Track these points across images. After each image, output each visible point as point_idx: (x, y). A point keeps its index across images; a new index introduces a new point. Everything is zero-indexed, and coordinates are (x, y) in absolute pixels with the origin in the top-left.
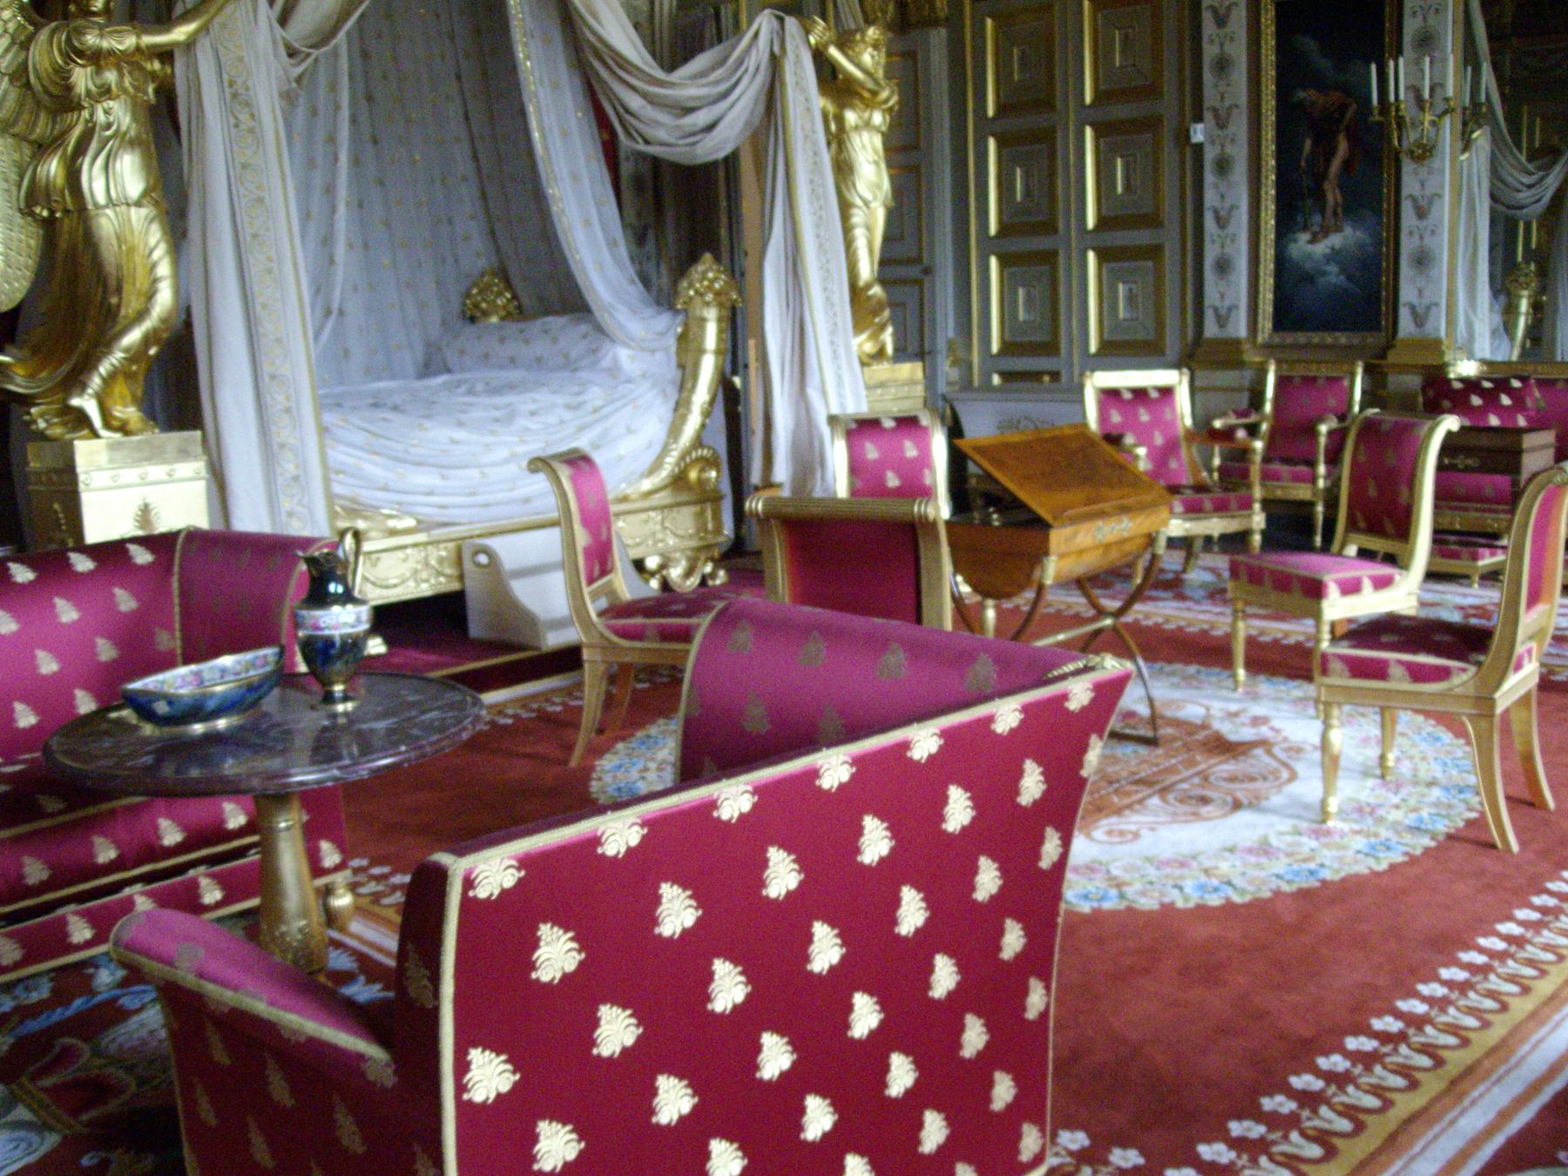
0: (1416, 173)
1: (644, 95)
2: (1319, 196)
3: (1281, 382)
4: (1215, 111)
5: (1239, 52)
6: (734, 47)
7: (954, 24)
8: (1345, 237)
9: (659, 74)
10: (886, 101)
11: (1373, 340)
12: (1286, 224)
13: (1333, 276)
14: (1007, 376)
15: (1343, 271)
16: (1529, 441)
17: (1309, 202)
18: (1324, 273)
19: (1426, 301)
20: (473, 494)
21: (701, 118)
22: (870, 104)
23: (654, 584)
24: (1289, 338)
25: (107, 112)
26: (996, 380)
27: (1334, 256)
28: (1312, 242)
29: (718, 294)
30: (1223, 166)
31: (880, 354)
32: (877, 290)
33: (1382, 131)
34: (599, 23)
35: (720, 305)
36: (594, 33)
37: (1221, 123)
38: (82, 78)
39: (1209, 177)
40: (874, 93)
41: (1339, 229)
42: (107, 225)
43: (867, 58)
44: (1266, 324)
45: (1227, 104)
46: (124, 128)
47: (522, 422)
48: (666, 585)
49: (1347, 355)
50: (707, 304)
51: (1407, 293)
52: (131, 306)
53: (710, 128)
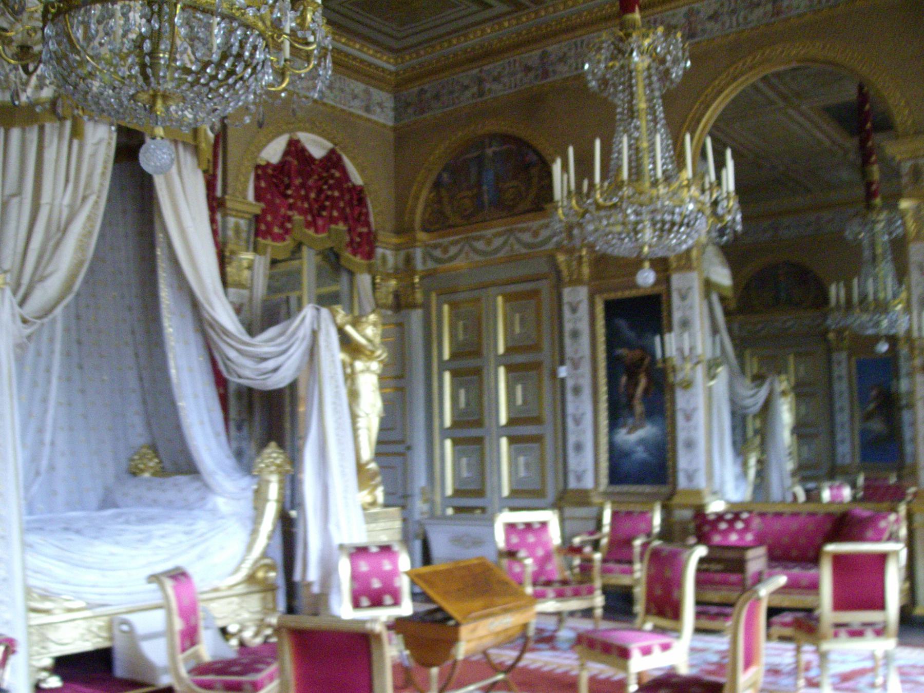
1: (238, 350)
2: (630, 406)
3: (615, 515)
5: (584, 326)
6: (290, 325)
7: (426, 306)
8: (647, 431)
9: (246, 338)
10: (379, 357)
11: (665, 490)
12: (614, 423)
13: (641, 454)
14: (458, 510)
16: (750, 554)
20: (121, 587)
21: (270, 364)
22: (370, 357)
23: (234, 642)
24: (618, 488)
26: (450, 511)
27: (641, 442)
29: (279, 466)
30: (577, 390)
31: (373, 504)
32: (373, 466)
33: (663, 373)
34: (213, 308)
35: (280, 473)
36: (208, 313)
37: (576, 365)
39: (569, 397)
40: (373, 352)
43: (370, 331)
44: (604, 480)
47: (156, 542)
48: (242, 644)
49: (651, 499)
50: (271, 472)
53: (275, 370)
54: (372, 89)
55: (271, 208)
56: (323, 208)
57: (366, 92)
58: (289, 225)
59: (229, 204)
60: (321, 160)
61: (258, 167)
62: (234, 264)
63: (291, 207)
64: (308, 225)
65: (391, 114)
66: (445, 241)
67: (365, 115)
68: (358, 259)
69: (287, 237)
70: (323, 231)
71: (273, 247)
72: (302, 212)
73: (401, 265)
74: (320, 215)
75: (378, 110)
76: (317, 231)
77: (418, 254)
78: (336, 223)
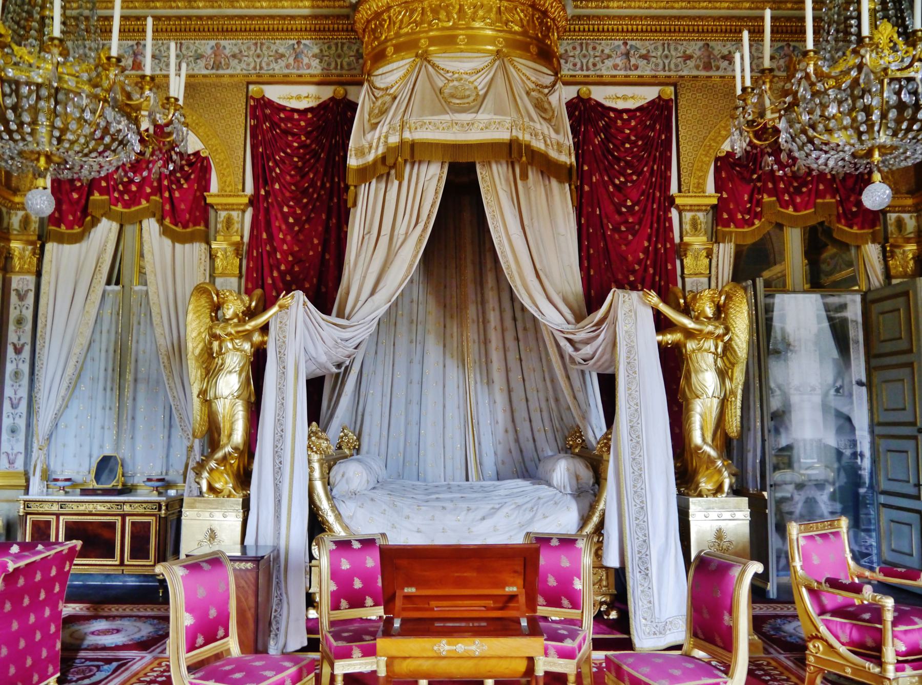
25: (222, 359)
38: (216, 345)
42: (222, 407)
46: (227, 365)
52: (224, 440)
55: (735, 196)
58: (759, 209)
59: (678, 201)
61: (717, 159)
62: (689, 254)
63: (760, 191)
64: (785, 205)
68: (855, 230)
69: (757, 222)
70: (806, 209)
72: (773, 192)
74: (798, 191)
76: (795, 210)
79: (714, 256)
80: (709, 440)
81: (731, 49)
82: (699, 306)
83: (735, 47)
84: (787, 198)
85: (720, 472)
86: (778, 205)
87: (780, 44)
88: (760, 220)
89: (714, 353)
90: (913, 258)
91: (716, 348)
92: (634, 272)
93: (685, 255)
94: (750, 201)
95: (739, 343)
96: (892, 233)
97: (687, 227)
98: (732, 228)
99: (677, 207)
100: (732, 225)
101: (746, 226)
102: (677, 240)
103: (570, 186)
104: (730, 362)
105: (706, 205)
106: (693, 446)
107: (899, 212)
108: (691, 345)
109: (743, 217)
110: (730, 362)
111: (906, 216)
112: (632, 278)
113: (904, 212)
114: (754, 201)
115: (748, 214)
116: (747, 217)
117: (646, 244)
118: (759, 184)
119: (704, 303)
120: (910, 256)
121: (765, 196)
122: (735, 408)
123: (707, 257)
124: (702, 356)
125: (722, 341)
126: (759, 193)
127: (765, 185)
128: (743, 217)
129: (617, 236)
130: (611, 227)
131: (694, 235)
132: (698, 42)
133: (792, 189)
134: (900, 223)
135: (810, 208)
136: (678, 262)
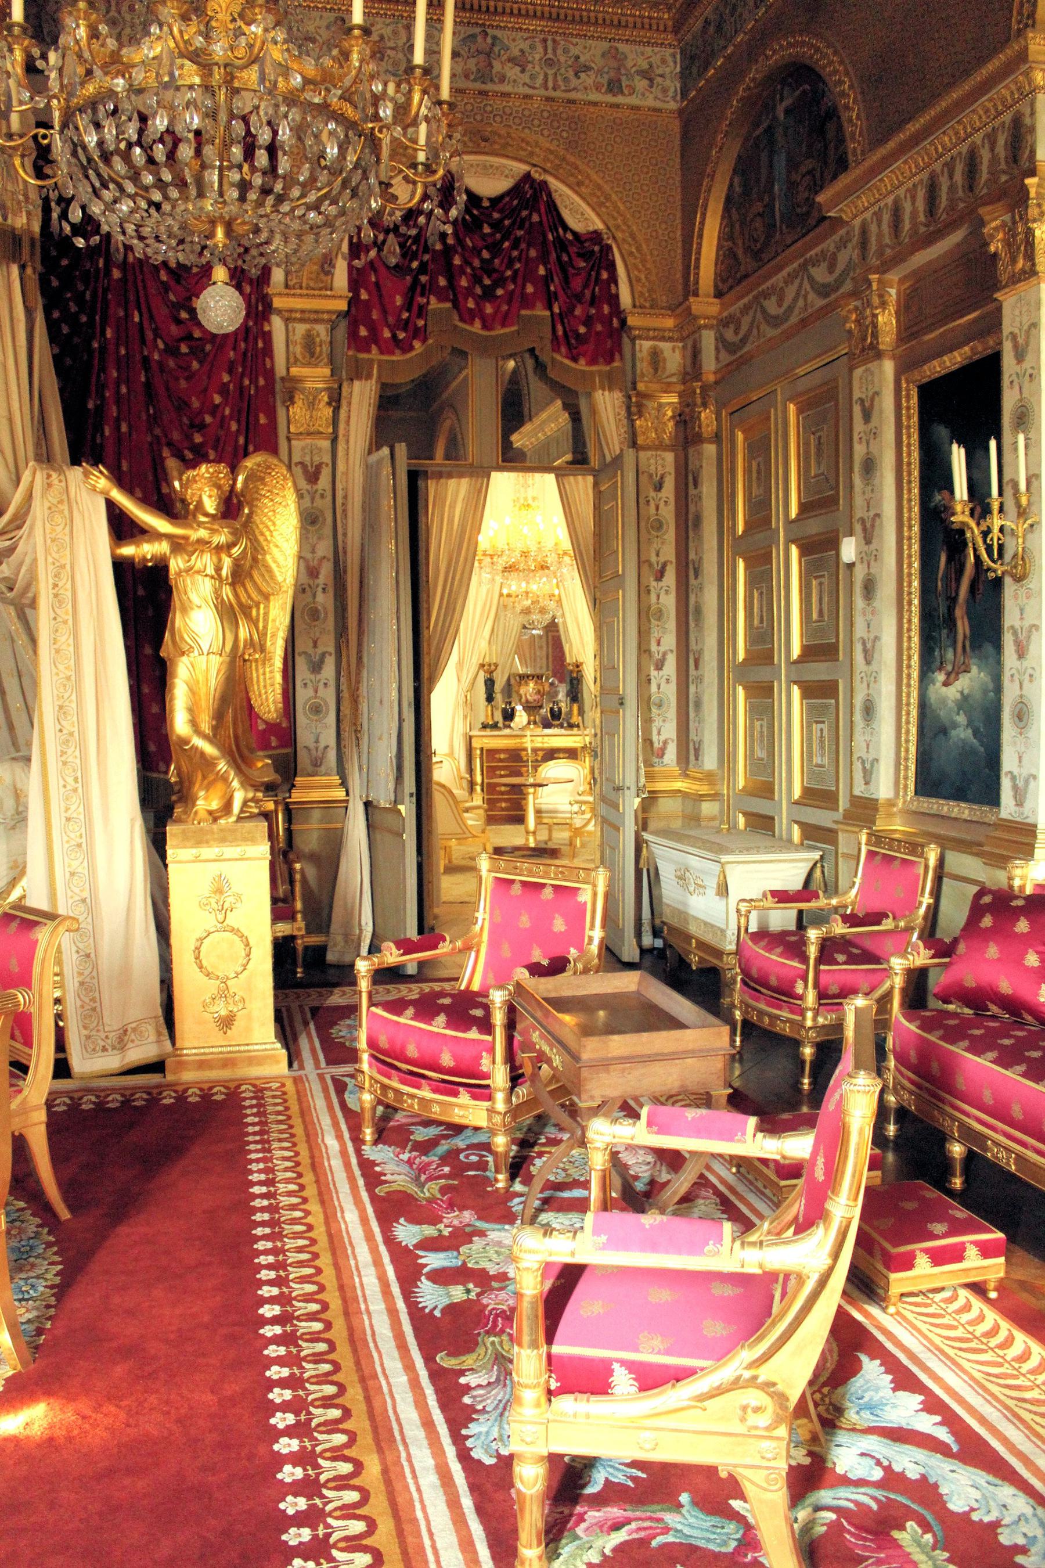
0: (1016, 597)
2: (950, 622)
4: (863, 521)
15: (970, 724)
17: (945, 632)
18: (955, 725)
19: (1025, 772)
26: (741, 820)
27: (964, 702)
28: (946, 684)
30: (869, 588)
41: (967, 671)
45: (872, 514)
51: (1008, 761)
54: (622, 47)
56: (500, 282)
57: (613, 54)
58: (421, 323)
60: (495, 201)
62: (299, 398)
64: (468, 317)
65: (674, 85)
66: (736, 308)
67: (610, 99)
68: (582, 365)
69: (417, 344)
70: (503, 325)
71: (379, 361)
73: (689, 370)
74: (488, 294)
75: (641, 84)
76: (485, 327)
77: (708, 340)
78: (532, 307)
79: (344, 402)
80: (206, 727)
81: (383, 31)
82: (193, 494)
83: (389, 29)
84: (471, 304)
85: (224, 779)
86: (456, 317)
87: (471, 30)
88: (424, 340)
89: (212, 577)
90: (673, 417)
91: (218, 569)
92: (201, 427)
93: (291, 400)
94: (408, 306)
95: (280, 559)
96: (643, 375)
97: (298, 350)
98: (375, 353)
99: (279, 312)
100: (374, 349)
101: (397, 351)
102: (280, 370)
103: (23, 268)
104: (260, 591)
105: (329, 312)
106: (173, 738)
107: (654, 338)
108: (176, 564)
109: (394, 336)
110: (260, 591)
111: (665, 346)
112: (198, 439)
113: (663, 339)
114: (415, 308)
115: (405, 329)
116: (401, 335)
117: (226, 378)
118: (423, 279)
119: (200, 489)
120: (670, 413)
121: (433, 300)
122: (271, 672)
123: (329, 404)
124: (193, 583)
125: (230, 556)
126: (422, 295)
127: (433, 281)
128: (394, 336)
129: (171, 363)
130: (161, 345)
131: (309, 364)
132: (324, 14)
133: (478, 291)
134: (656, 357)
135: (512, 325)
136: (281, 413)
